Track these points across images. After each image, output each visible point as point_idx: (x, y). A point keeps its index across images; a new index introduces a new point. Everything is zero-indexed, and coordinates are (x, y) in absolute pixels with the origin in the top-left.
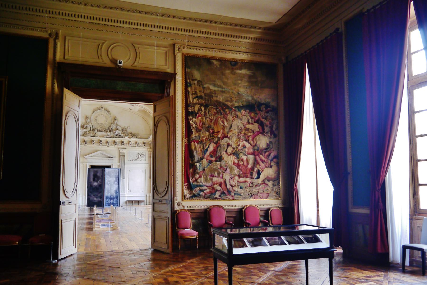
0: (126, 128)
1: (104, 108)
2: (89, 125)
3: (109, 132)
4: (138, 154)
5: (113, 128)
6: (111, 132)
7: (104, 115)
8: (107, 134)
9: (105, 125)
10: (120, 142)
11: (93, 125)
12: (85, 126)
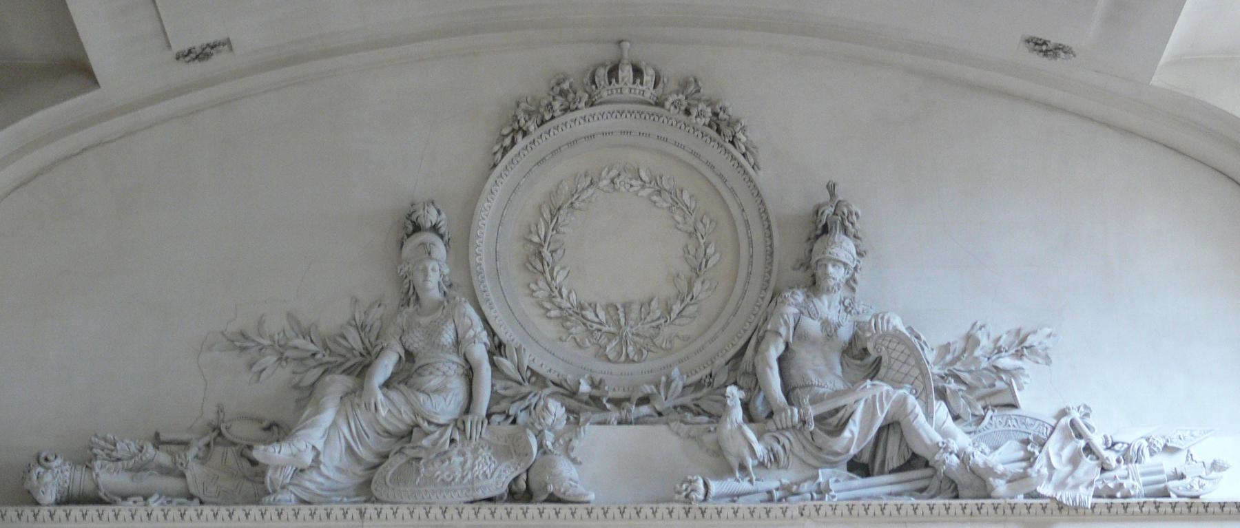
1: (649, 77)
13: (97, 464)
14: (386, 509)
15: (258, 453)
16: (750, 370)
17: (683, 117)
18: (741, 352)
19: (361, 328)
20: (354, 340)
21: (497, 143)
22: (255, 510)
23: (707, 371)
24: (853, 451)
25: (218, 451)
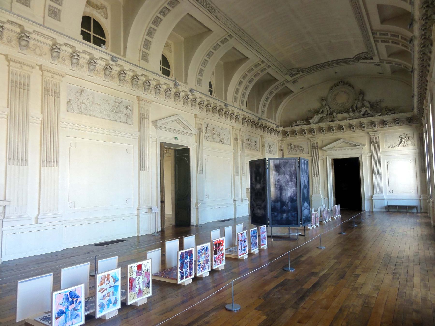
1: (343, 82)
5: (359, 106)
8: (350, 115)
10: (370, 123)
11: (330, 107)
20: (318, 110)
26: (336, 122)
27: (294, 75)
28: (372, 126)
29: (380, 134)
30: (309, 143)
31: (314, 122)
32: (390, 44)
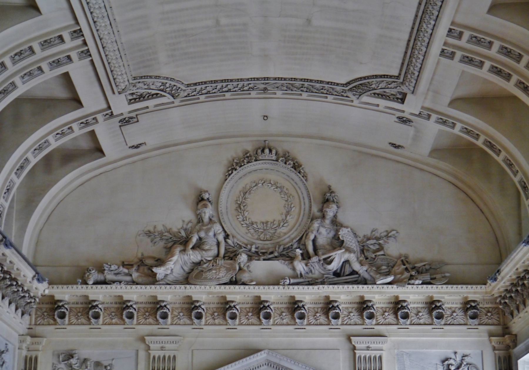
0: (378, 239)
1: (274, 152)
2: (211, 234)
3: (303, 259)
4: (443, 362)
6: (309, 258)
7: (276, 185)
8: (294, 269)
9: (284, 230)
10: (356, 306)
12: (194, 239)
13: (106, 272)
14: (193, 286)
15: (155, 270)
16: (304, 243)
17: (284, 165)
18: (301, 238)
19: (185, 230)
20: (183, 234)
21: (227, 172)
22: (153, 287)
23: (290, 244)
24: (335, 269)
25: (141, 268)
26: (247, 287)
27: (141, 98)
28: (361, 315)
29: (384, 346)
30: (142, 354)
31: (171, 278)
32: (484, 73)
